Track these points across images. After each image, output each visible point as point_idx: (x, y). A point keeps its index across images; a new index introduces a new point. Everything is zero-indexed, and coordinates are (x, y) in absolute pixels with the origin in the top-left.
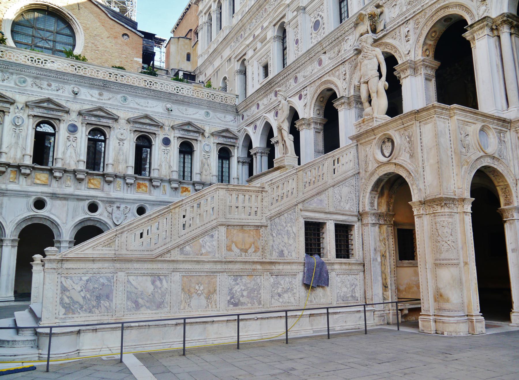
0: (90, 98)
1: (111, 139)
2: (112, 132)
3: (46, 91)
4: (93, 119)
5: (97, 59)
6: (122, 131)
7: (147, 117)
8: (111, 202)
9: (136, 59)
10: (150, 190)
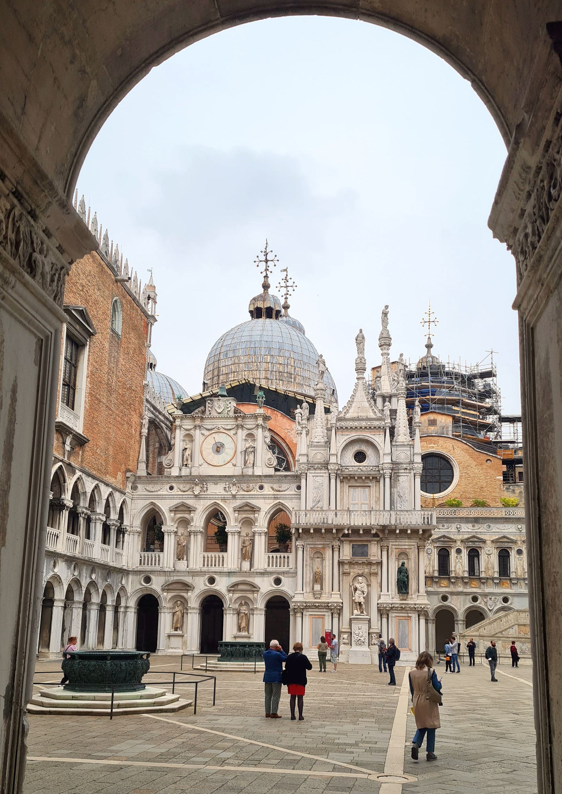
0: (467, 529)
1: (482, 555)
2: (483, 550)
3: (442, 530)
4: (470, 543)
5: (470, 484)
6: (489, 548)
7: (504, 537)
8: (485, 595)
9: (497, 478)
10: (511, 587)
